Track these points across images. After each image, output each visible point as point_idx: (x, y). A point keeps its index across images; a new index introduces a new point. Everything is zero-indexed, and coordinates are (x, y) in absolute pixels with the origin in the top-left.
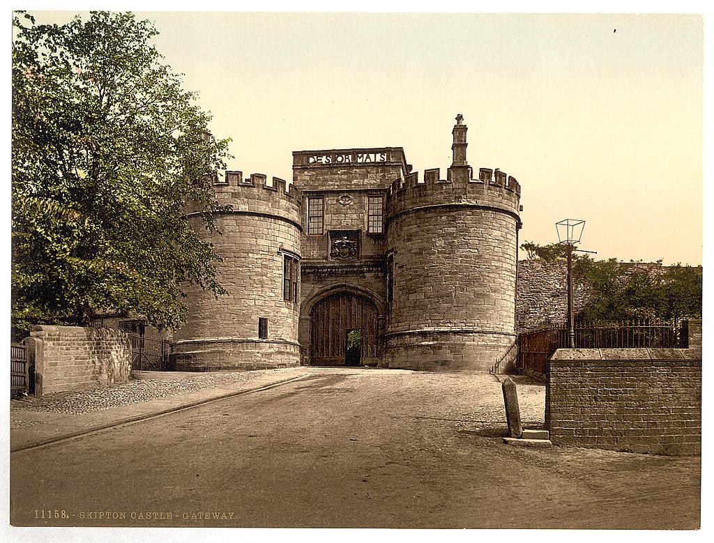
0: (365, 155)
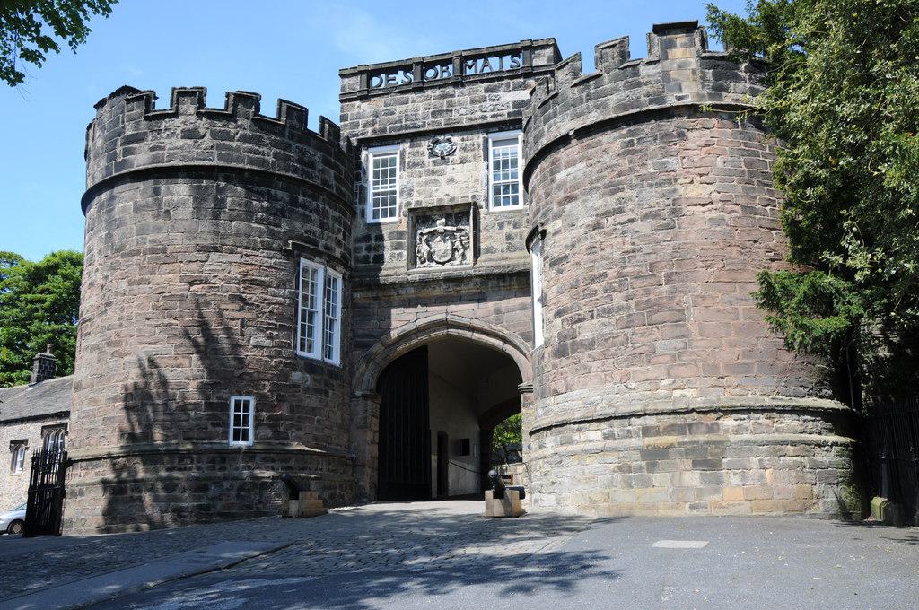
0: (480, 62)
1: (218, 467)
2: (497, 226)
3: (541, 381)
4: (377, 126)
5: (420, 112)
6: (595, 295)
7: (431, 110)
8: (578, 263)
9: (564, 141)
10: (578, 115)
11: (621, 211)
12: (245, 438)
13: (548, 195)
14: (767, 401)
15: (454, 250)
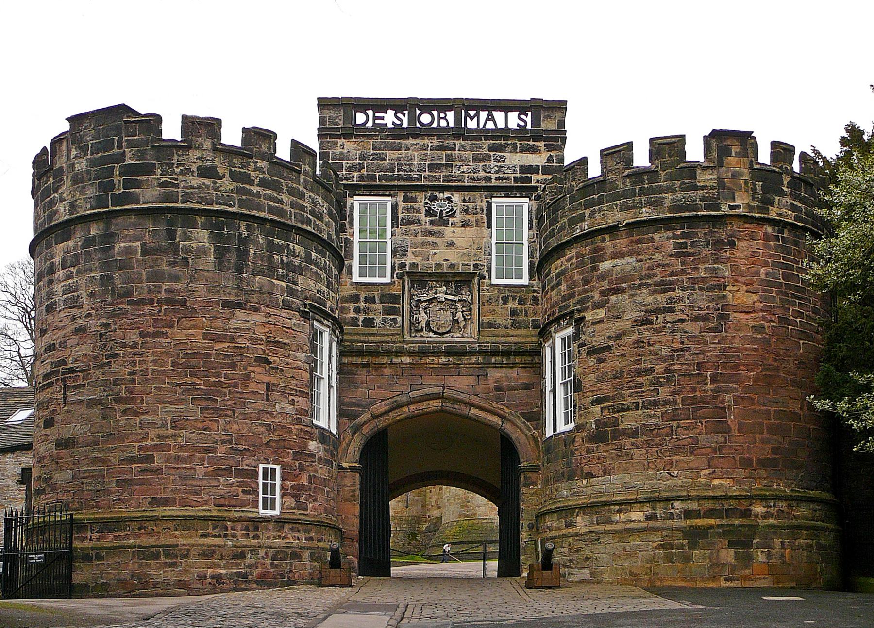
0: (484, 115)
1: (251, 535)
2: (501, 301)
3: (569, 464)
4: (364, 172)
5: (415, 163)
6: (641, 387)
7: (428, 163)
8: (623, 355)
12: (273, 508)
13: (586, 282)
15: (455, 321)
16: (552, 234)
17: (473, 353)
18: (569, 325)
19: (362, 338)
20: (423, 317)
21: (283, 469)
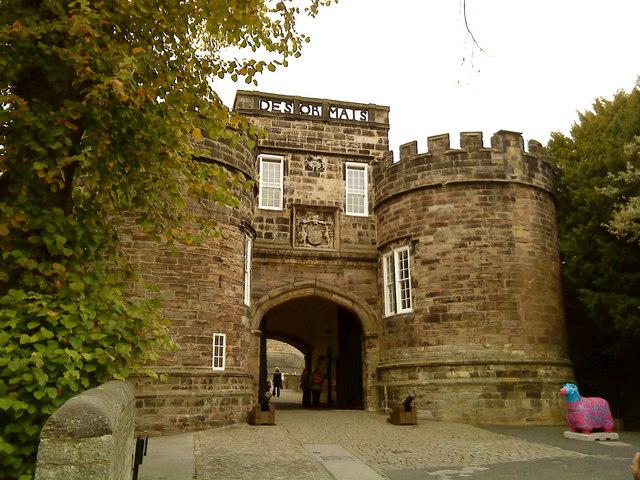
0: (340, 111)
9: (438, 187)
10: (448, 174)
11: (479, 239)
14: (555, 360)
16: (391, 187)
17: (335, 259)
18: (405, 244)
19: (267, 246)
20: (304, 234)
21: (227, 336)
